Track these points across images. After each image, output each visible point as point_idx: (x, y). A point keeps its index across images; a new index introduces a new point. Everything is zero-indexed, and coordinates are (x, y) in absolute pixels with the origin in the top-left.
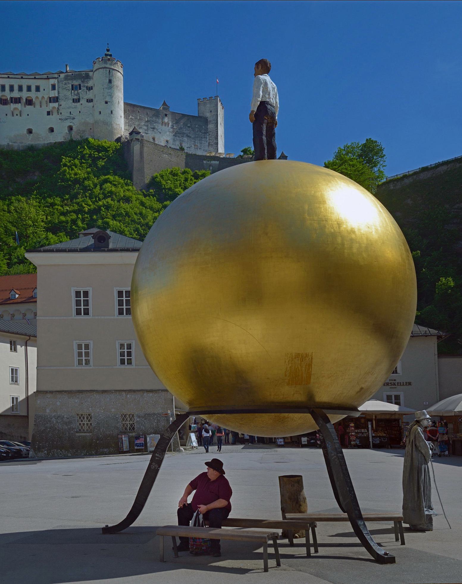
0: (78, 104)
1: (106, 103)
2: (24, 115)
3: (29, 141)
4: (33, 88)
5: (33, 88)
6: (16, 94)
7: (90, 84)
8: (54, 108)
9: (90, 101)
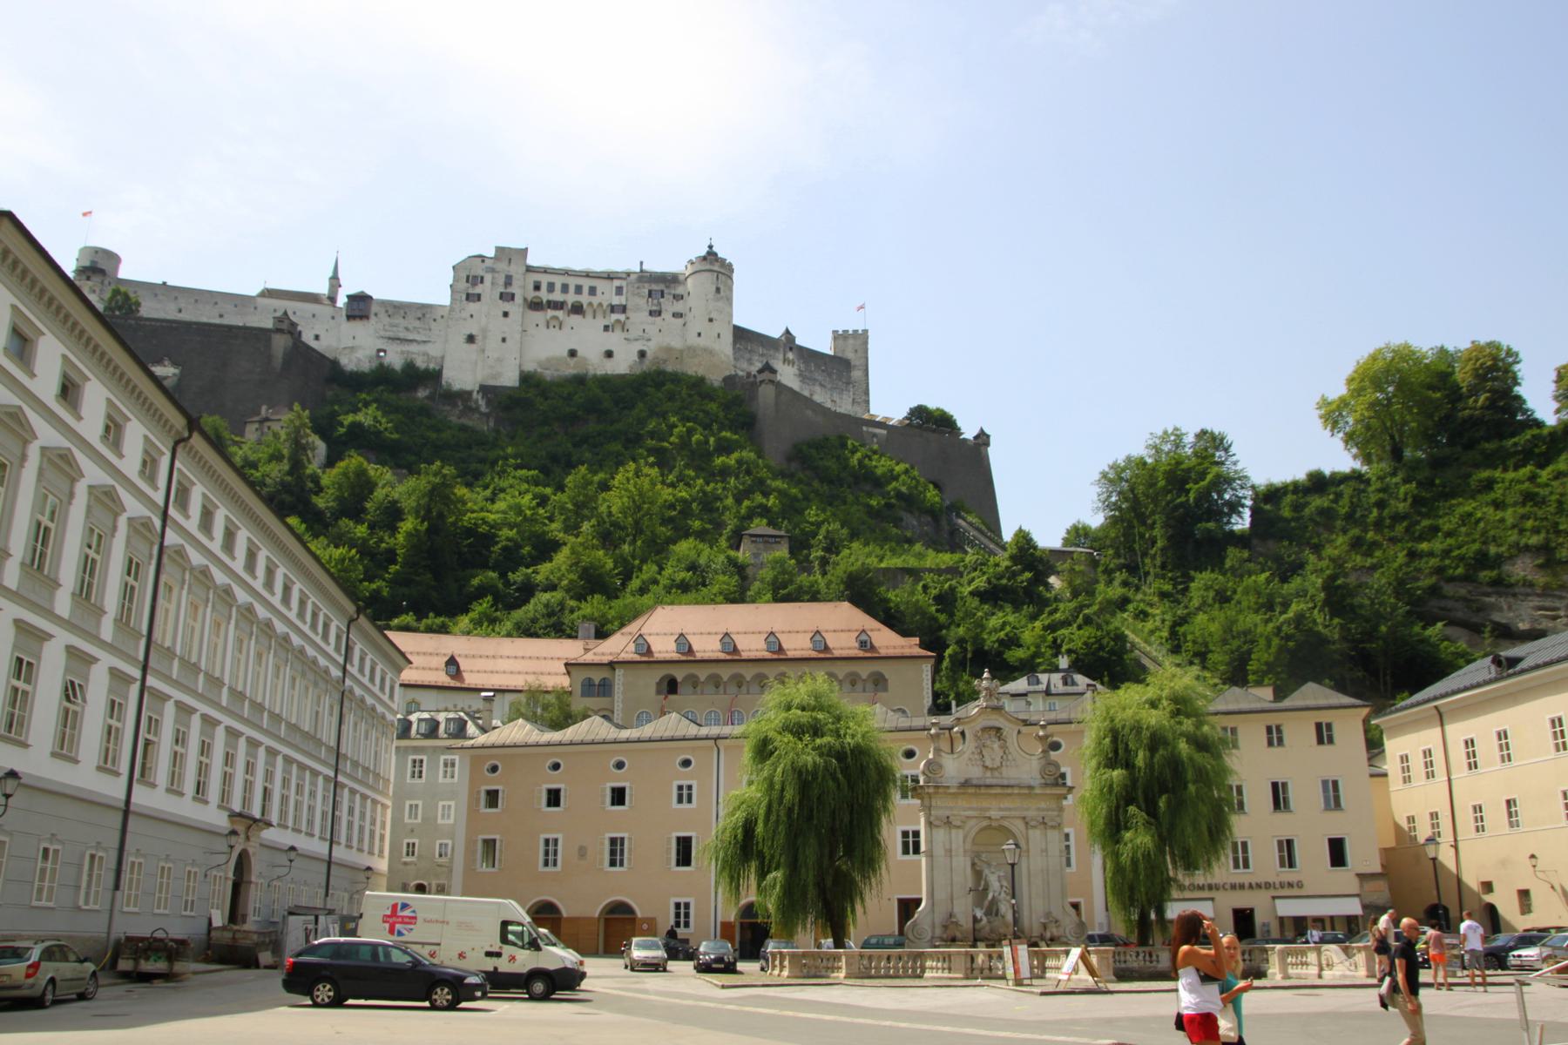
0: (658, 319)
1: (711, 320)
2: (566, 329)
3: (570, 369)
4: (586, 290)
5: (586, 290)
6: (557, 296)
7: (680, 290)
8: (618, 321)
9: (675, 315)
